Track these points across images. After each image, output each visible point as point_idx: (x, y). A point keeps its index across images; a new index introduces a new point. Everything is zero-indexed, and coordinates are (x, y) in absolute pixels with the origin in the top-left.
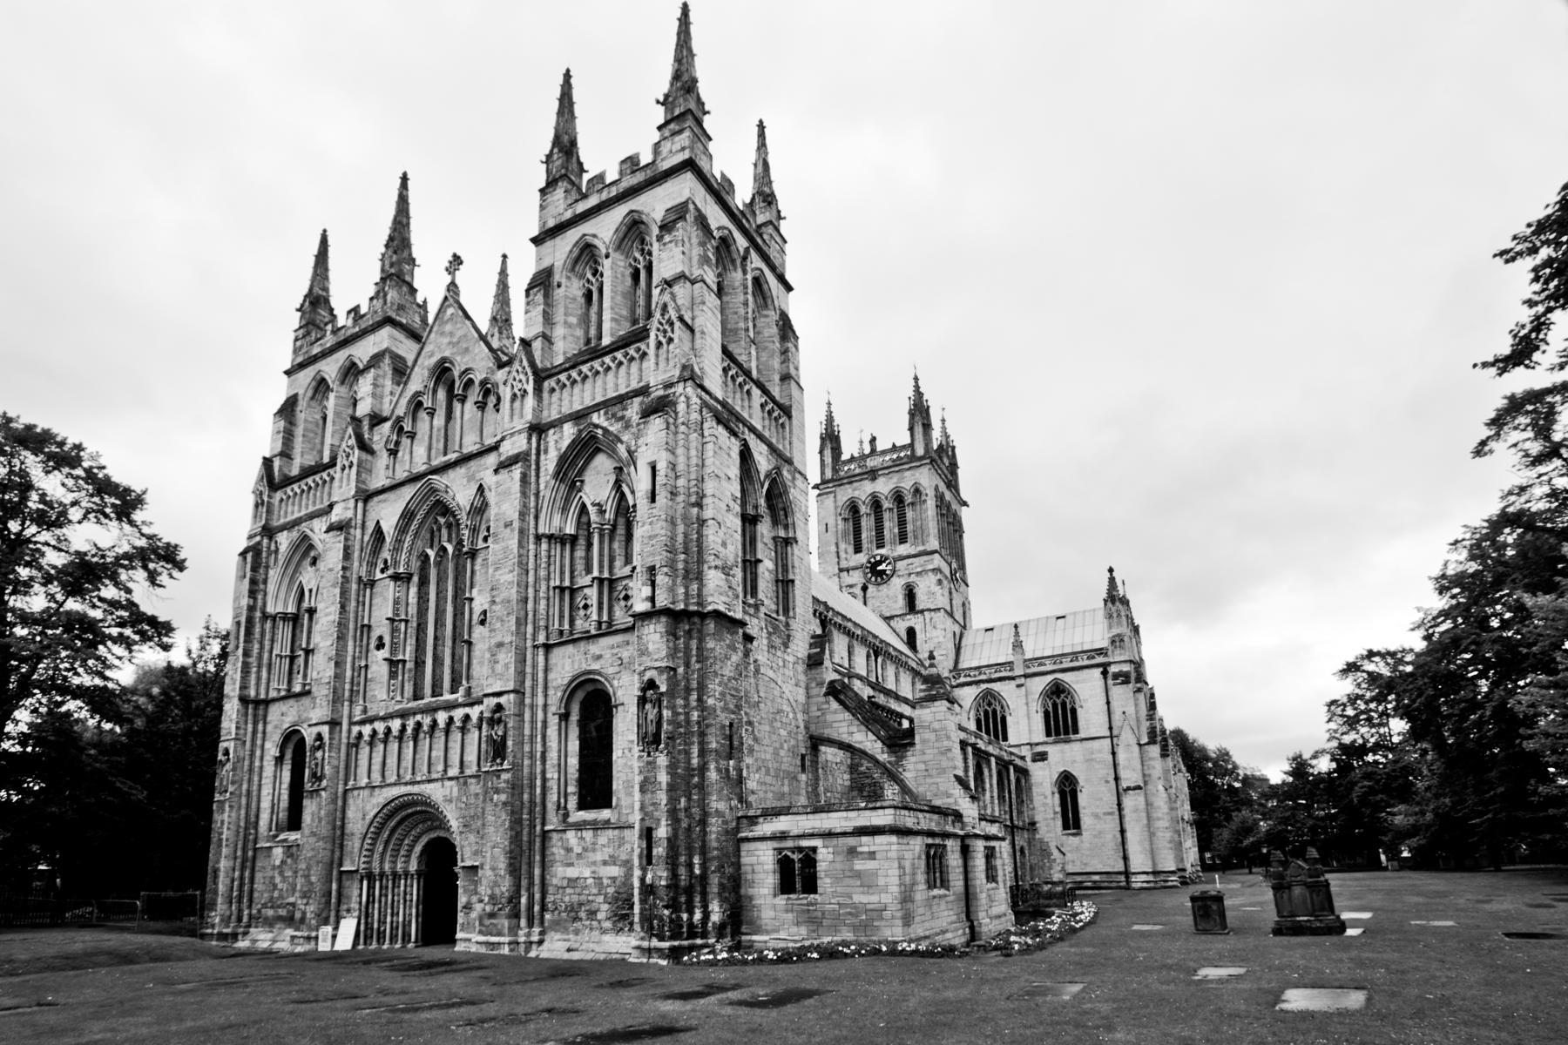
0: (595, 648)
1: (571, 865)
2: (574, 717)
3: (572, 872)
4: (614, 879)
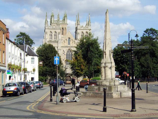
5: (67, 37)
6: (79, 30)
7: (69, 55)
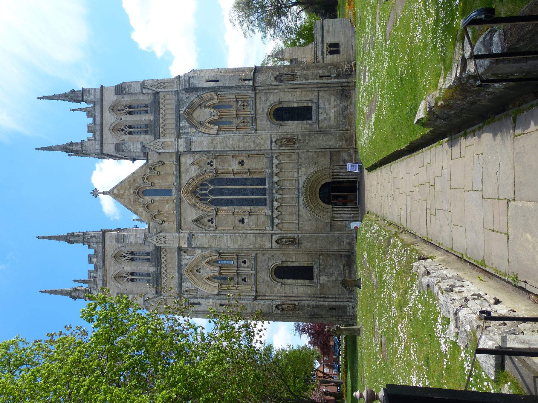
0: (260, 111)
1: (330, 117)
2: (281, 122)
3: (332, 117)
4: (335, 100)
5: (135, 201)
6: (106, 142)
7: (220, 192)
